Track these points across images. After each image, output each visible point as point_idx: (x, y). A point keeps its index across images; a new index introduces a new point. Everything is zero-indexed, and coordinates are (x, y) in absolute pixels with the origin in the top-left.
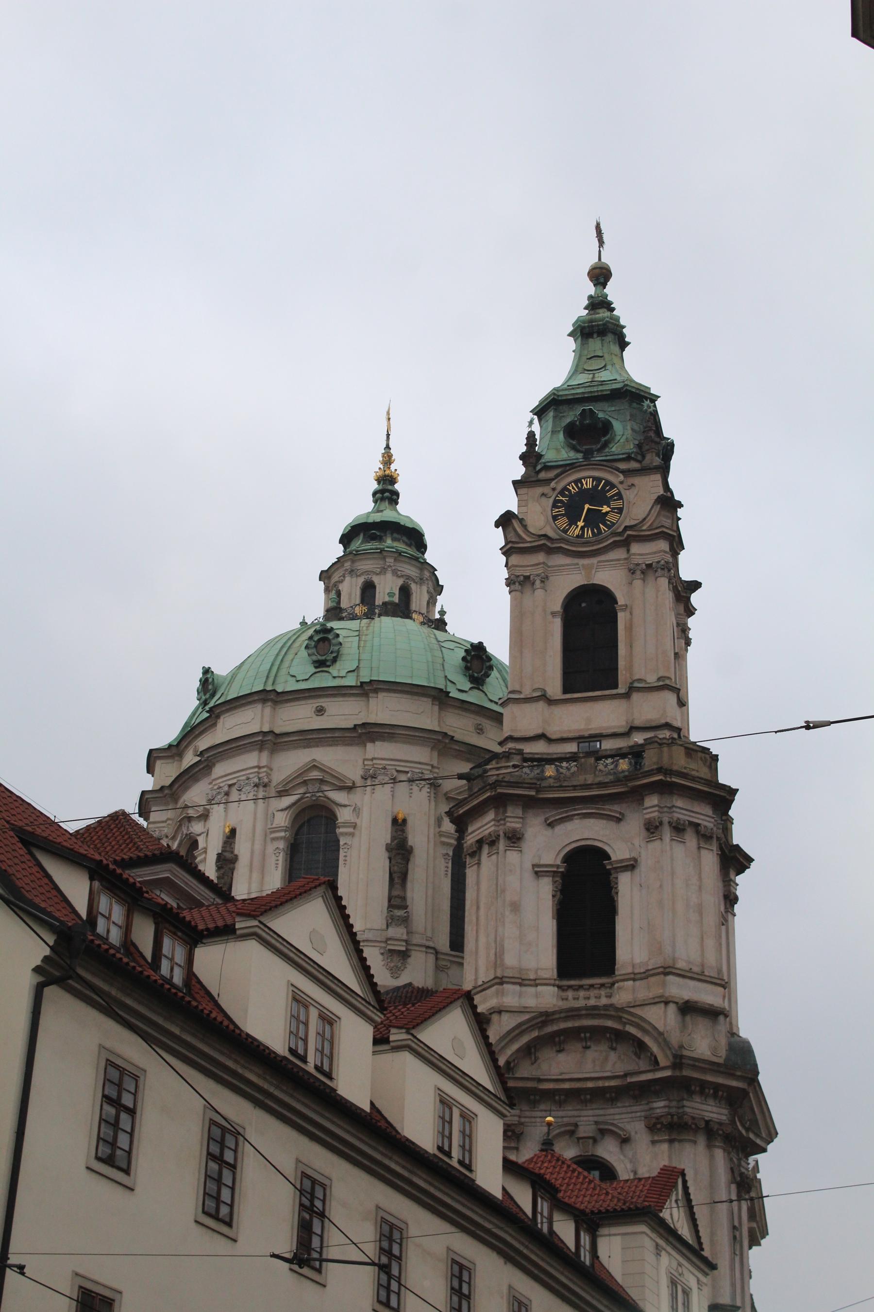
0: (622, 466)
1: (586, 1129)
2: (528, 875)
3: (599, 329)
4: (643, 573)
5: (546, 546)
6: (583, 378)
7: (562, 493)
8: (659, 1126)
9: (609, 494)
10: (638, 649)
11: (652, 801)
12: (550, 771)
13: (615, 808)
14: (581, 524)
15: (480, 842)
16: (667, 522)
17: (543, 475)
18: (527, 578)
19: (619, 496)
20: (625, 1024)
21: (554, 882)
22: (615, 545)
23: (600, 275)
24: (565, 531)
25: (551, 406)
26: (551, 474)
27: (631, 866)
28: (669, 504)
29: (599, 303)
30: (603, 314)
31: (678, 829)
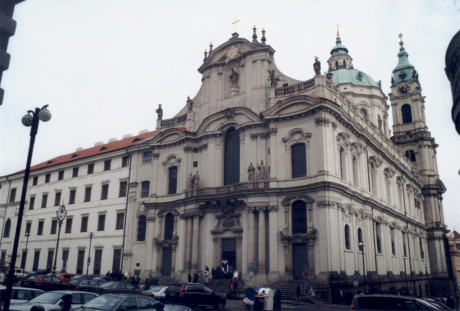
0: (409, 81)
3: (403, 55)
5: (397, 98)
6: (400, 65)
10: (415, 116)
13: (414, 143)
16: (418, 91)
19: (409, 87)
23: (401, 44)
25: (395, 71)
26: (397, 85)
27: (417, 153)
28: (419, 88)
29: (402, 49)
30: (403, 51)
31: (425, 146)
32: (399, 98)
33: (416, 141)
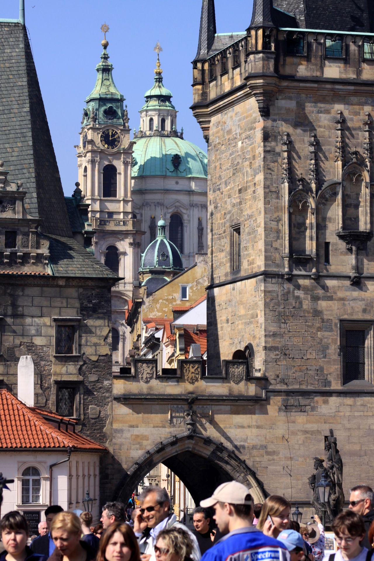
24: (104, 146)
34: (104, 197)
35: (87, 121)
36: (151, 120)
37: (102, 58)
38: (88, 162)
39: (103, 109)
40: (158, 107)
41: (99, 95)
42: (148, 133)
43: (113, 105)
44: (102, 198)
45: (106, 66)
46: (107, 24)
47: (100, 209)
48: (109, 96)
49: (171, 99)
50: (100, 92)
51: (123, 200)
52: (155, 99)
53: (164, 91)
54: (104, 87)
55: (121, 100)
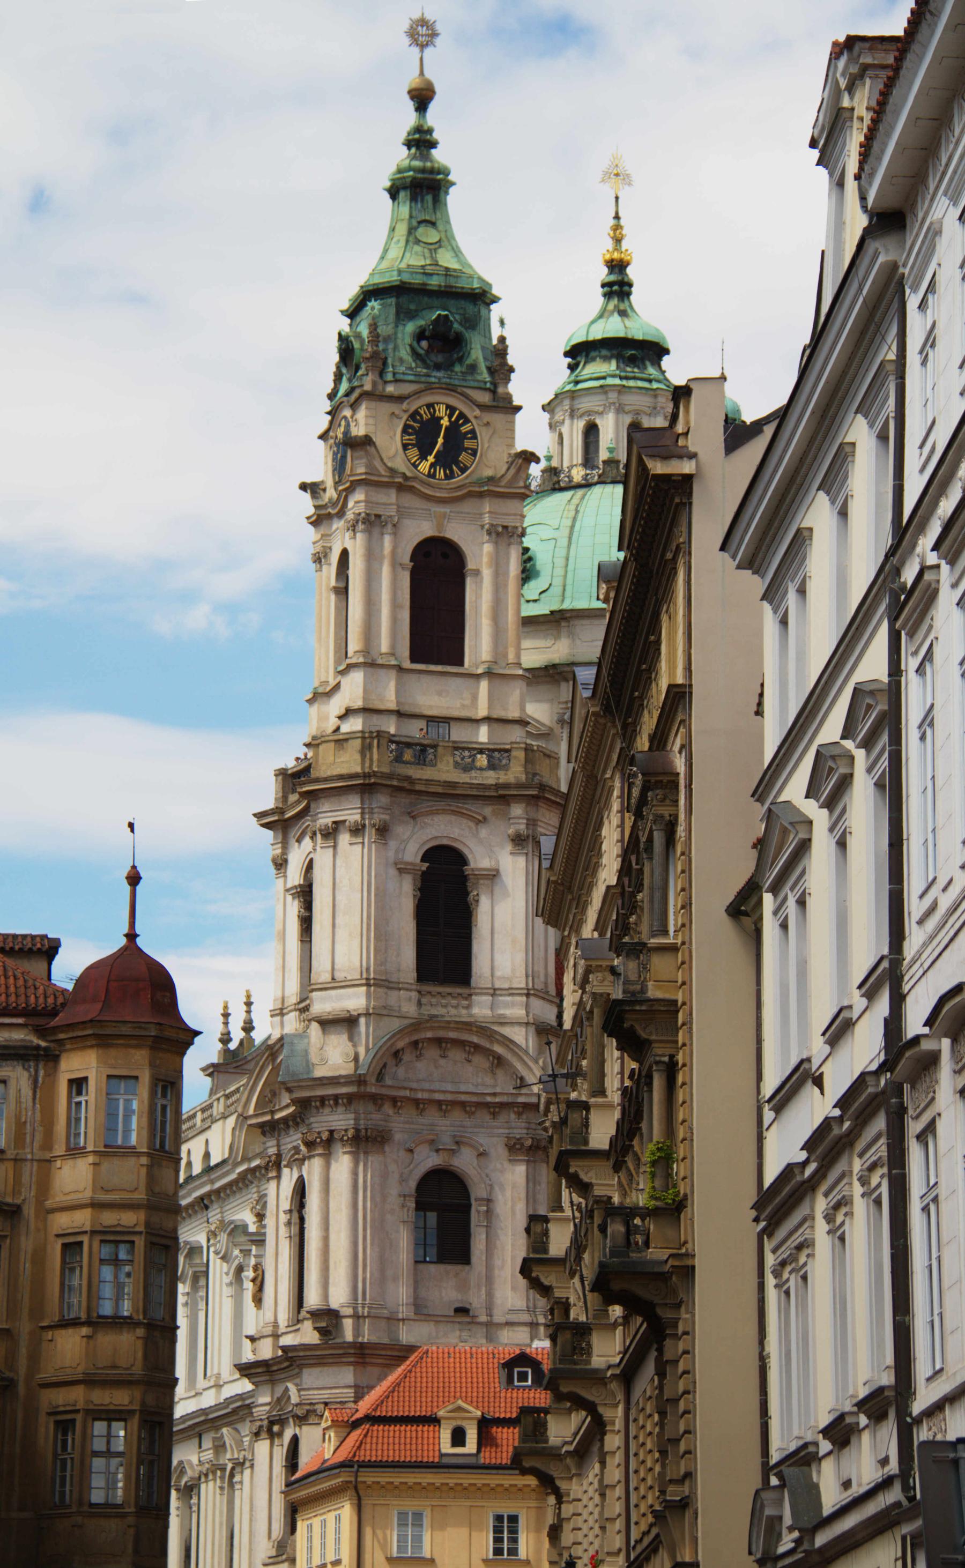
1: (446, 1141)
2: (393, 872)
4: (498, 534)
7: (414, 415)
8: (518, 1146)
9: (464, 429)
11: (517, 810)
12: (408, 755)
14: (431, 459)
15: (338, 825)
17: (390, 389)
18: (378, 516)
20: (492, 1042)
21: (414, 880)
22: (470, 495)
24: (415, 466)
32: (411, 489)
33: (501, 797)
34: (413, 659)
35: (350, 380)
36: (591, 431)
37: (409, 144)
38: (353, 528)
39: (411, 327)
40: (617, 381)
41: (400, 272)
42: (578, 474)
43: (453, 313)
44: (407, 664)
45: (423, 170)
46: (429, 16)
47: (398, 703)
48: (434, 282)
49: (666, 362)
50: (403, 265)
51: (489, 674)
52: (604, 352)
53: (635, 329)
54: (417, 248)
55: (481, 298)
